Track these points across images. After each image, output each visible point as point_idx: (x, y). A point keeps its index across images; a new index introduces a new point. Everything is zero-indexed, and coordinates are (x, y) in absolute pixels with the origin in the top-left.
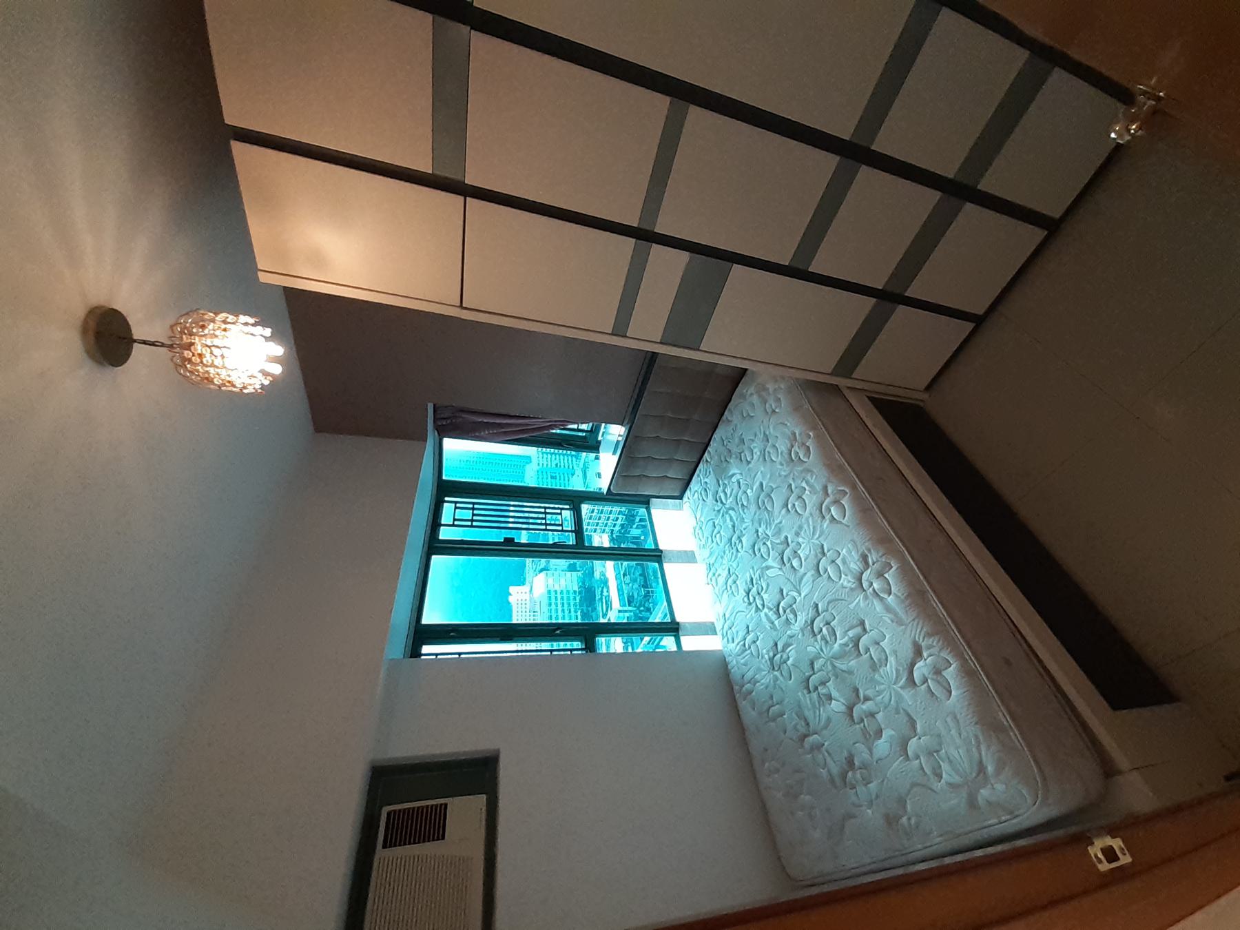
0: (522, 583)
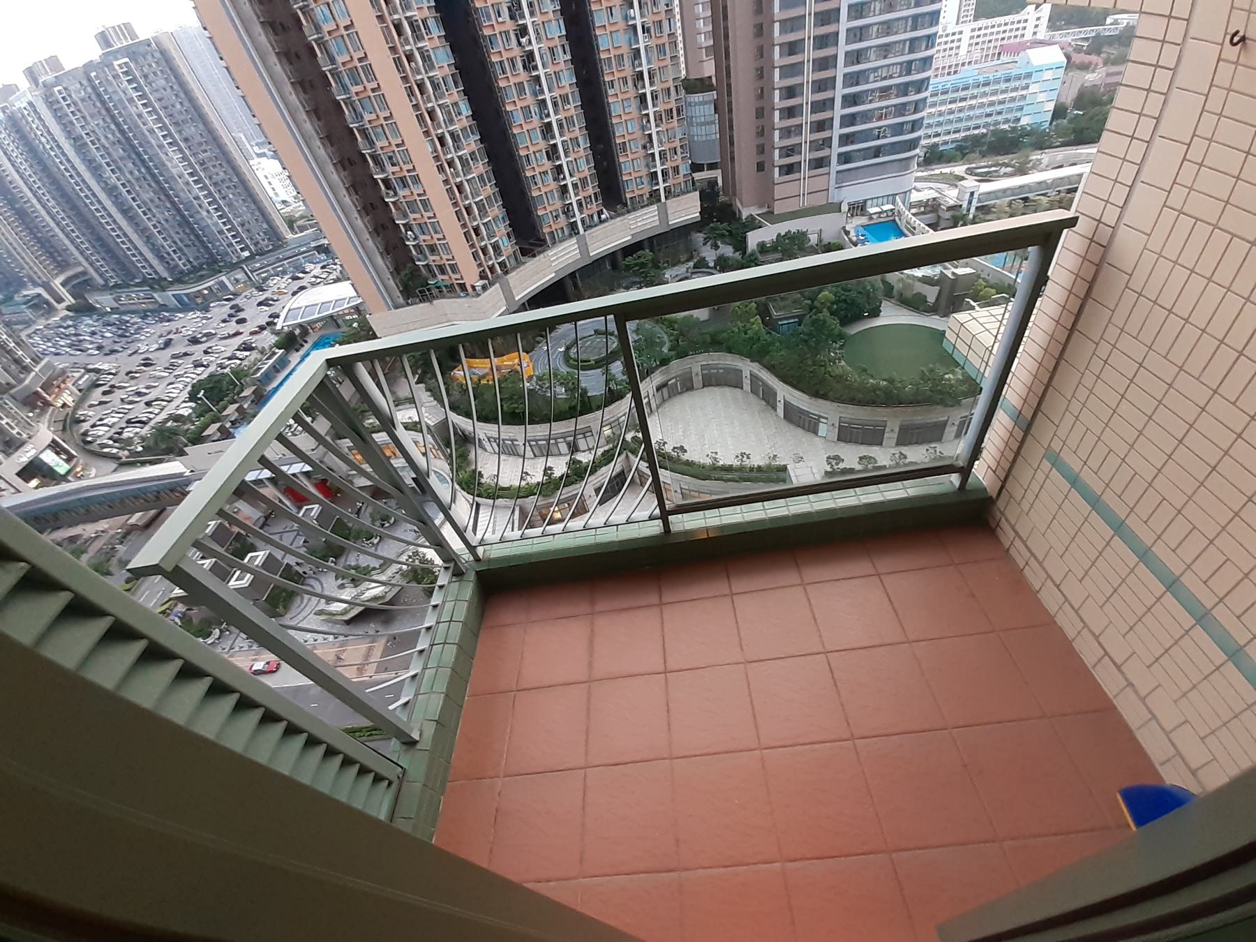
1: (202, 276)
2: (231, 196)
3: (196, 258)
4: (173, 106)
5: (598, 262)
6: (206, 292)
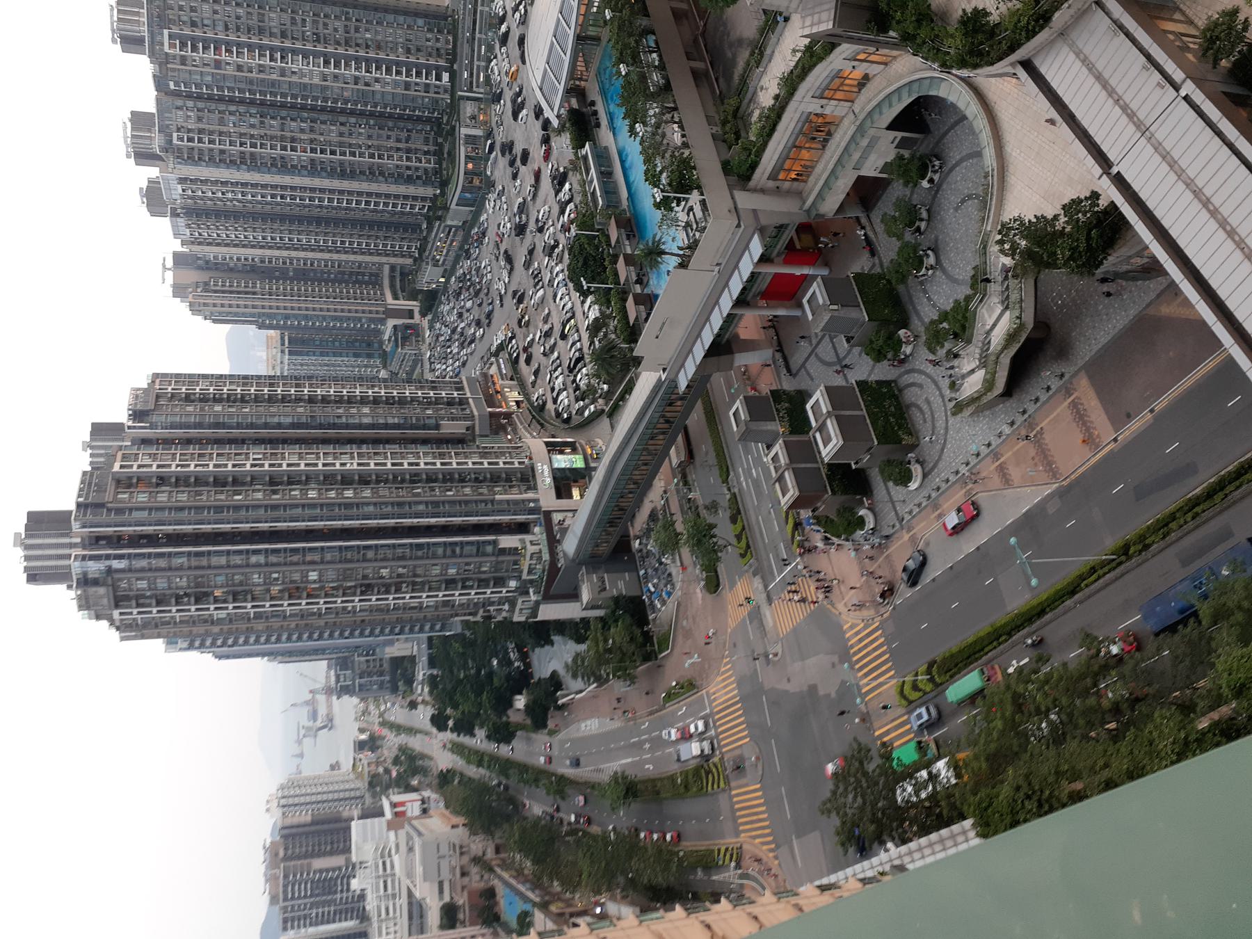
1: (449, 153)
2: (368, 36)
3: (426, 141)
4: (238, 18)
6: (470, 166)
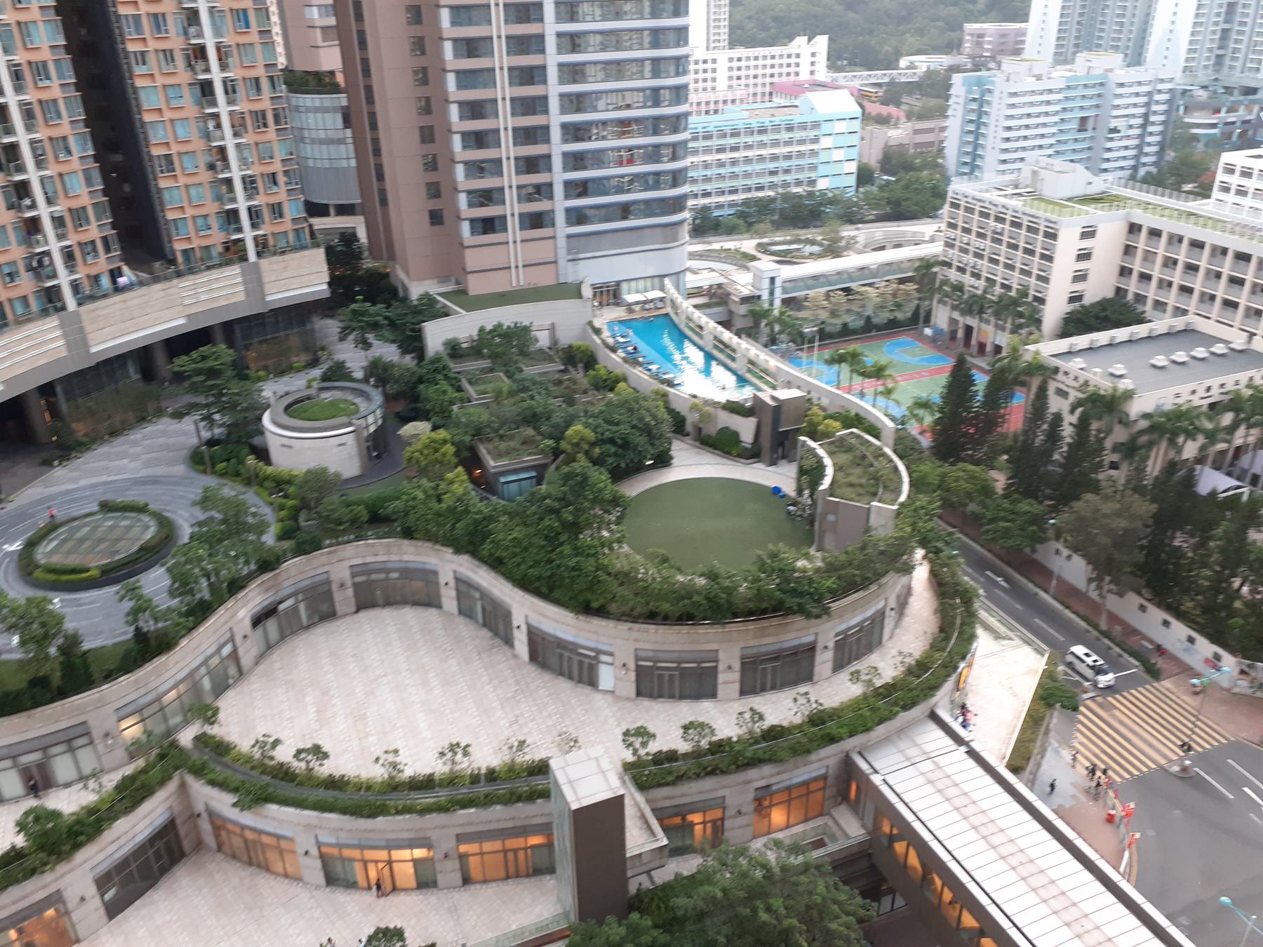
0: (835, 61)
5: (112, 366)
